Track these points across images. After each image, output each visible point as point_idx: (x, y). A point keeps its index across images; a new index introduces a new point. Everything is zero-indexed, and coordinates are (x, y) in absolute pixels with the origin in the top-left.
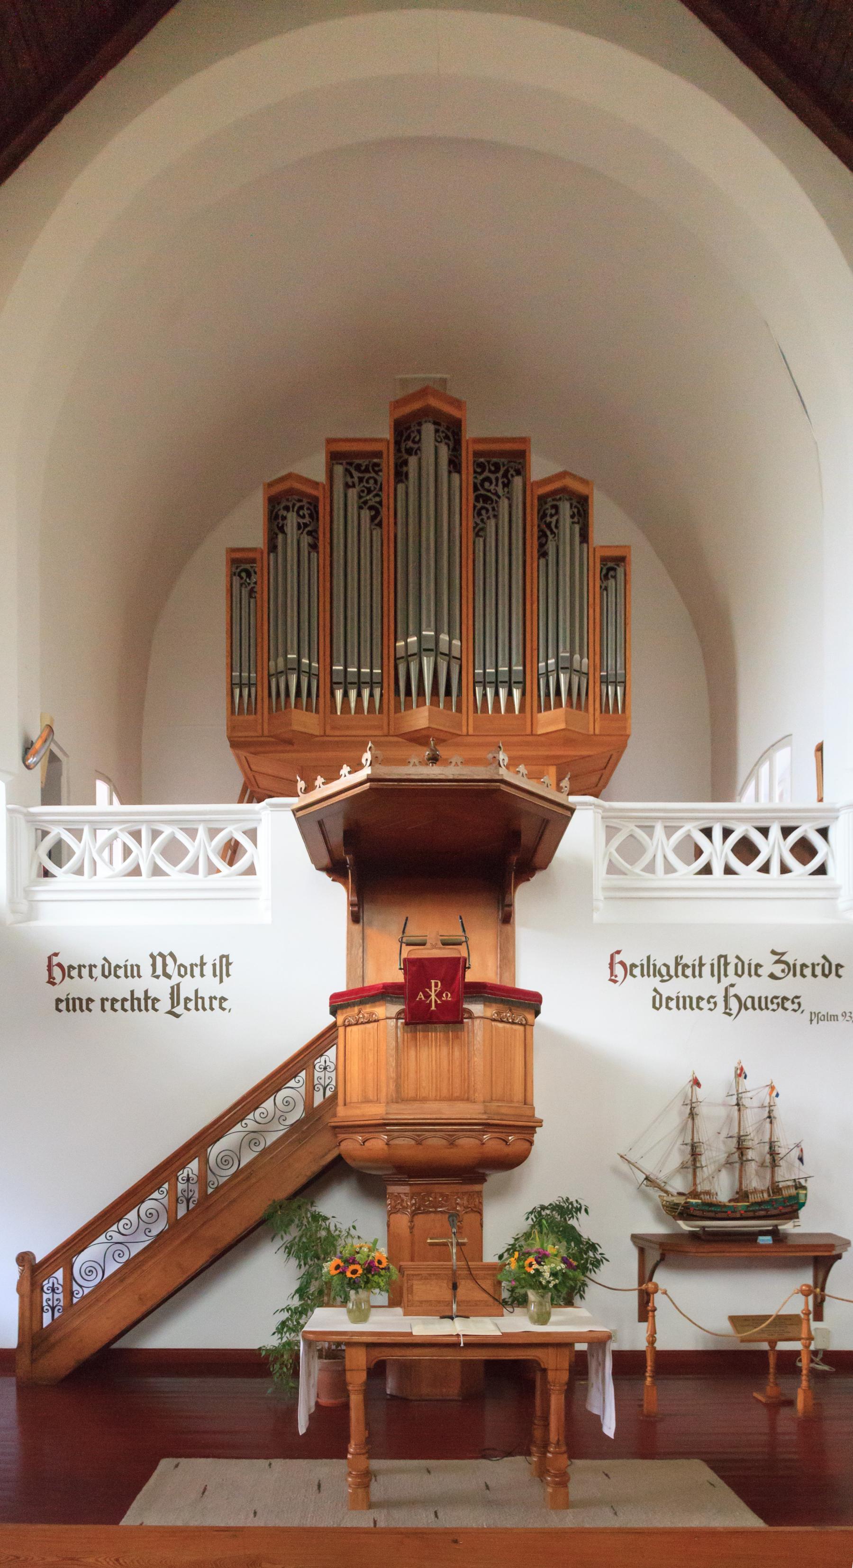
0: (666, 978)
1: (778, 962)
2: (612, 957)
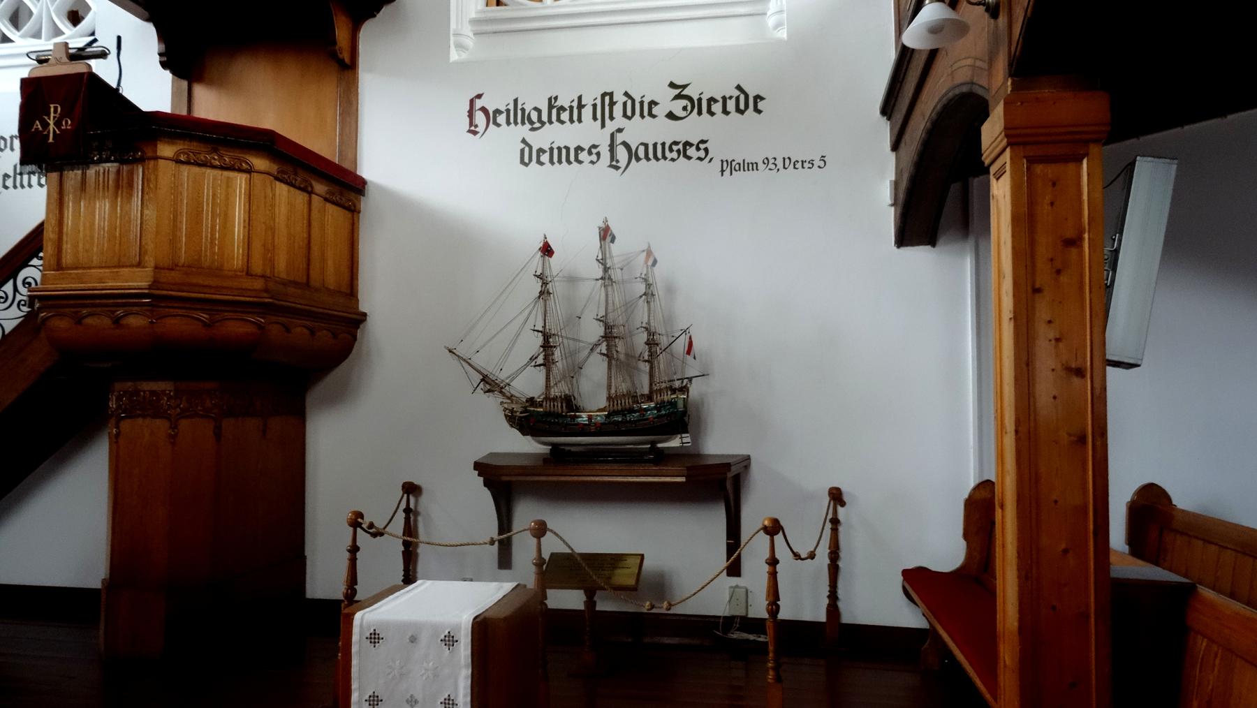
0: (537, 125)
1: (678, 97)
2: (472, 102)
